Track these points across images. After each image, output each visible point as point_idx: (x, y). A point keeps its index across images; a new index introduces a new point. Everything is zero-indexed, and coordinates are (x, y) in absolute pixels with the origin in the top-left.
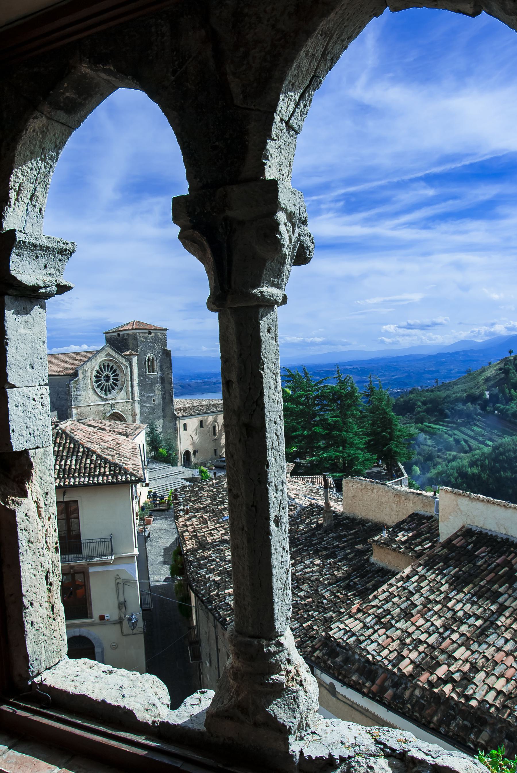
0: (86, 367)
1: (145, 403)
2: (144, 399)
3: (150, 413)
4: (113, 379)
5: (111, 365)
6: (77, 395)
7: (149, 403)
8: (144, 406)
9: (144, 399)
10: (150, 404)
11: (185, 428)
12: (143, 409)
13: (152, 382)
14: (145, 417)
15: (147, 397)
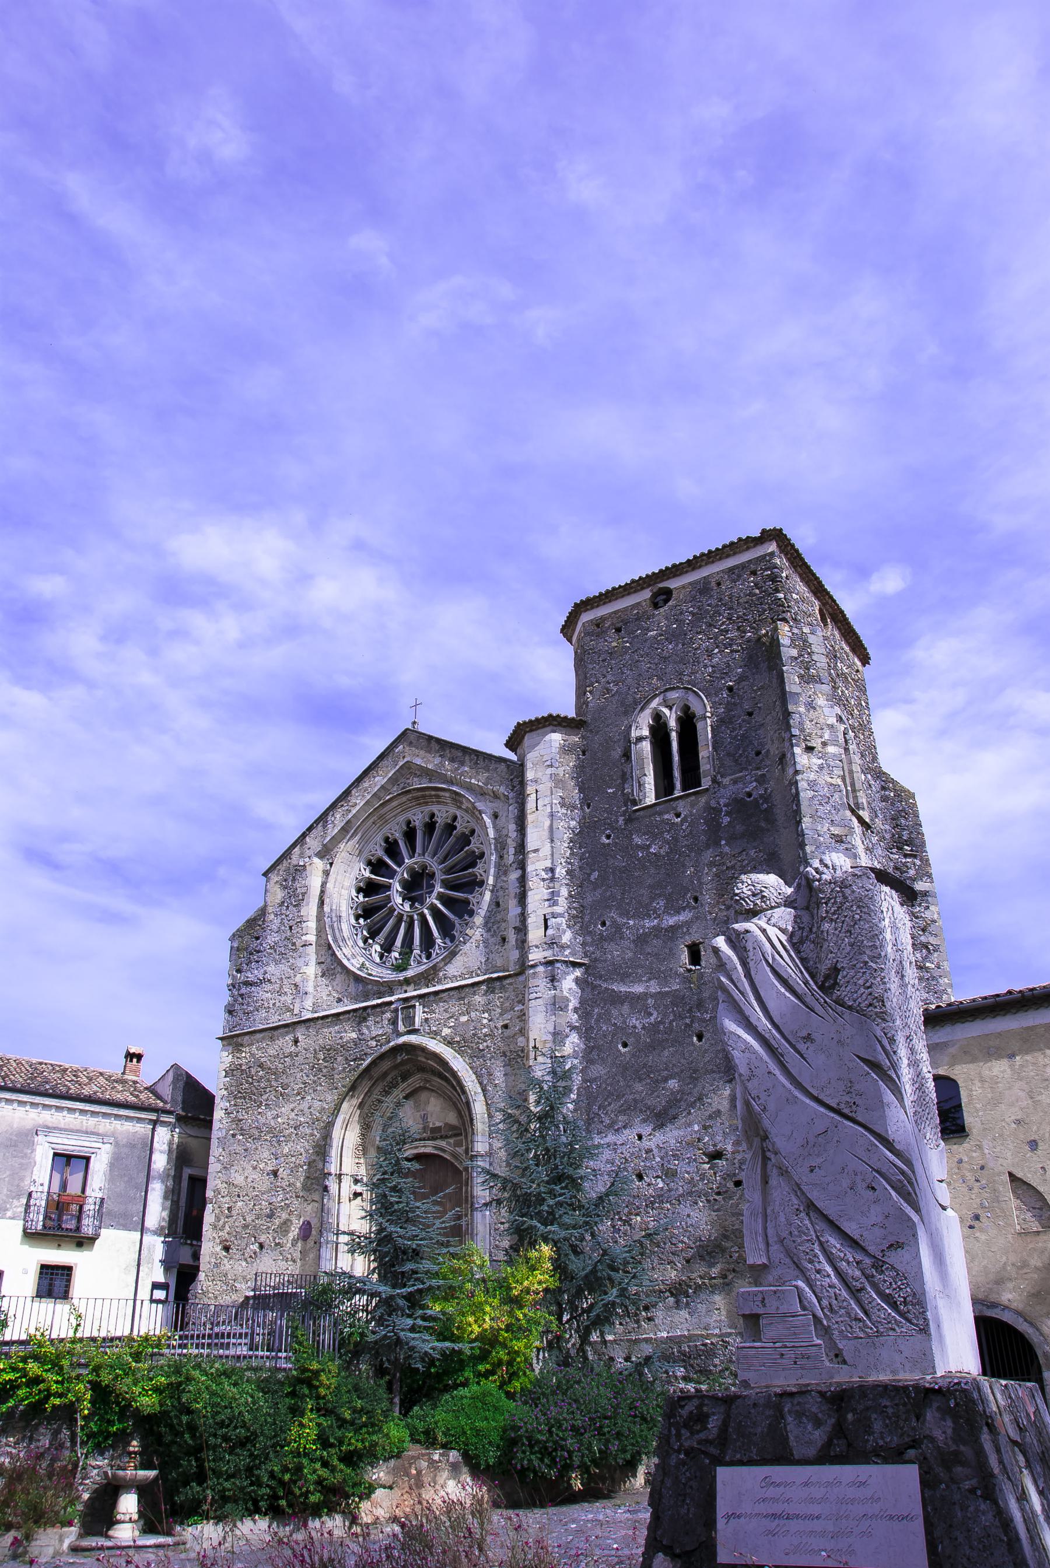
0: (302, 855)
1: (624, 978)
2: (615, 952)
3: (657, 1038)
4: (392, 874)
5: (440, 820)
6: (247, 983)
7: (654, 975)
8: (617, 999)
9: (615, 952)
10: (663, 977)
11: (952, 1124)
12: (605, 1017)
13: (675, 839)
14: (625, 1068)
15: (641, 940)
